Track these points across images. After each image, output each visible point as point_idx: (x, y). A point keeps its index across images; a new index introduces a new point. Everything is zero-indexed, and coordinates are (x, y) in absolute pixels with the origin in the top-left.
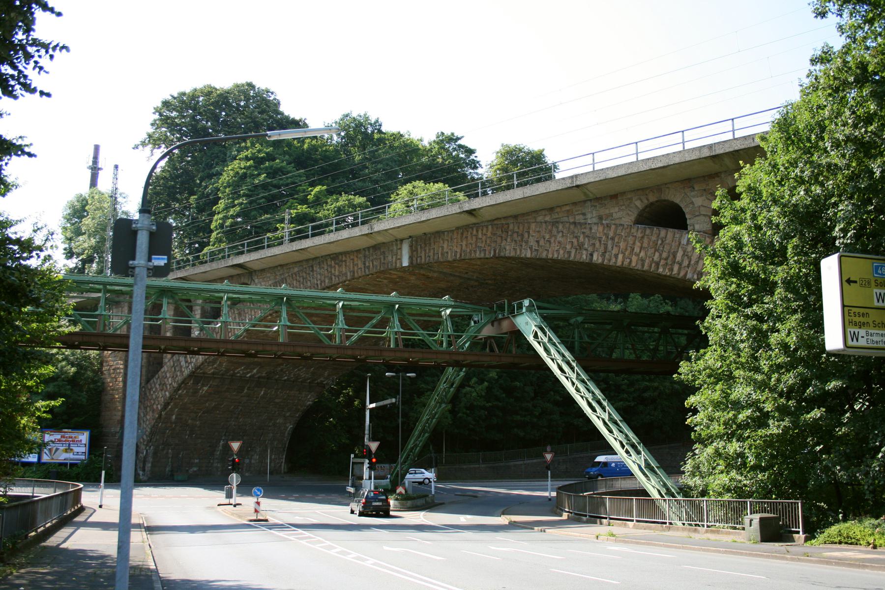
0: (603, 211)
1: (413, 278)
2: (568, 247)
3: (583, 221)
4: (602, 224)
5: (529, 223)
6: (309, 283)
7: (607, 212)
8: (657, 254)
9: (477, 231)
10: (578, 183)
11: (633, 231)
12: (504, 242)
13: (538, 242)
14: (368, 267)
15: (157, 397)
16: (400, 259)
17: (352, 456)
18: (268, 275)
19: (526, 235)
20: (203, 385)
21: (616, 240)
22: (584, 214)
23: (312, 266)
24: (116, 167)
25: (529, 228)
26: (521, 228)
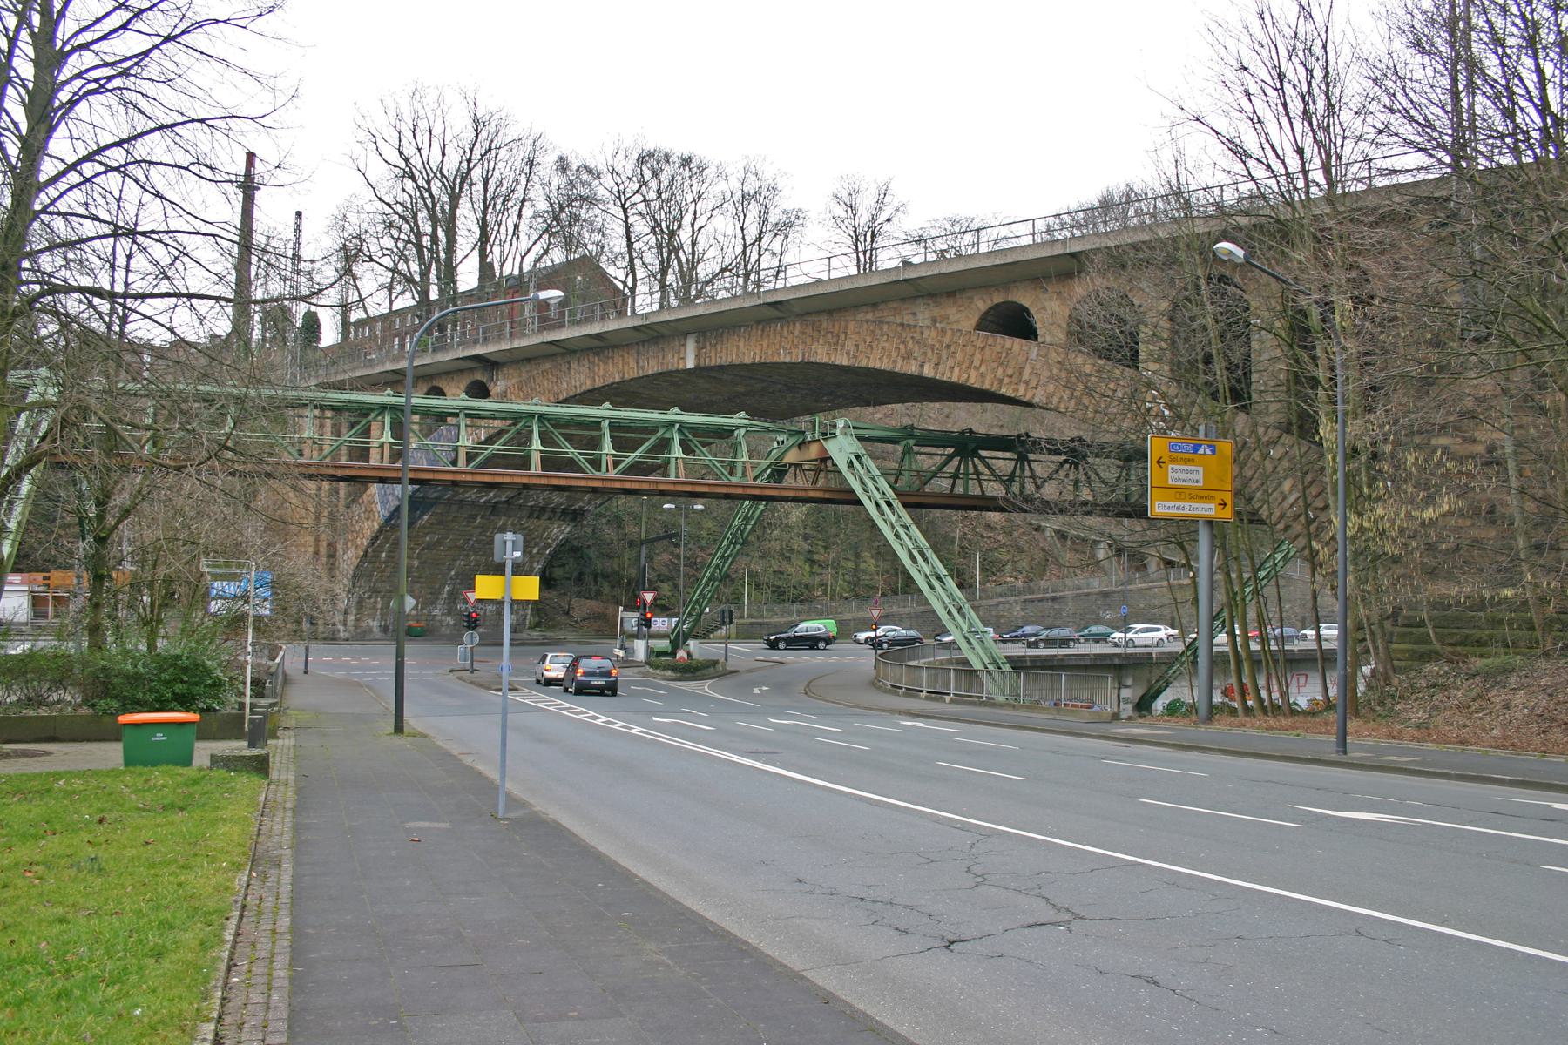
0: (937, 312)
1: (701, 381)
2: (894, 354)
3: (912, 323)
4: (936, 328)
5: (846, 321)
6: (565, 384)
7: (943, 313)
8: (1000, 370)
9: (782, 327)
10: (907, 277)
11: (973, 338)
12: (815, 345)
13: (857, 346)
14: (643, 368)
15: (362, 529)
17: (621, 609)
19: (842, 337)
20: (423, 513)
21: (952, 349)
22: (914, 314)
23: (569, 363)
24: (299, 214)
25: (846, 328)
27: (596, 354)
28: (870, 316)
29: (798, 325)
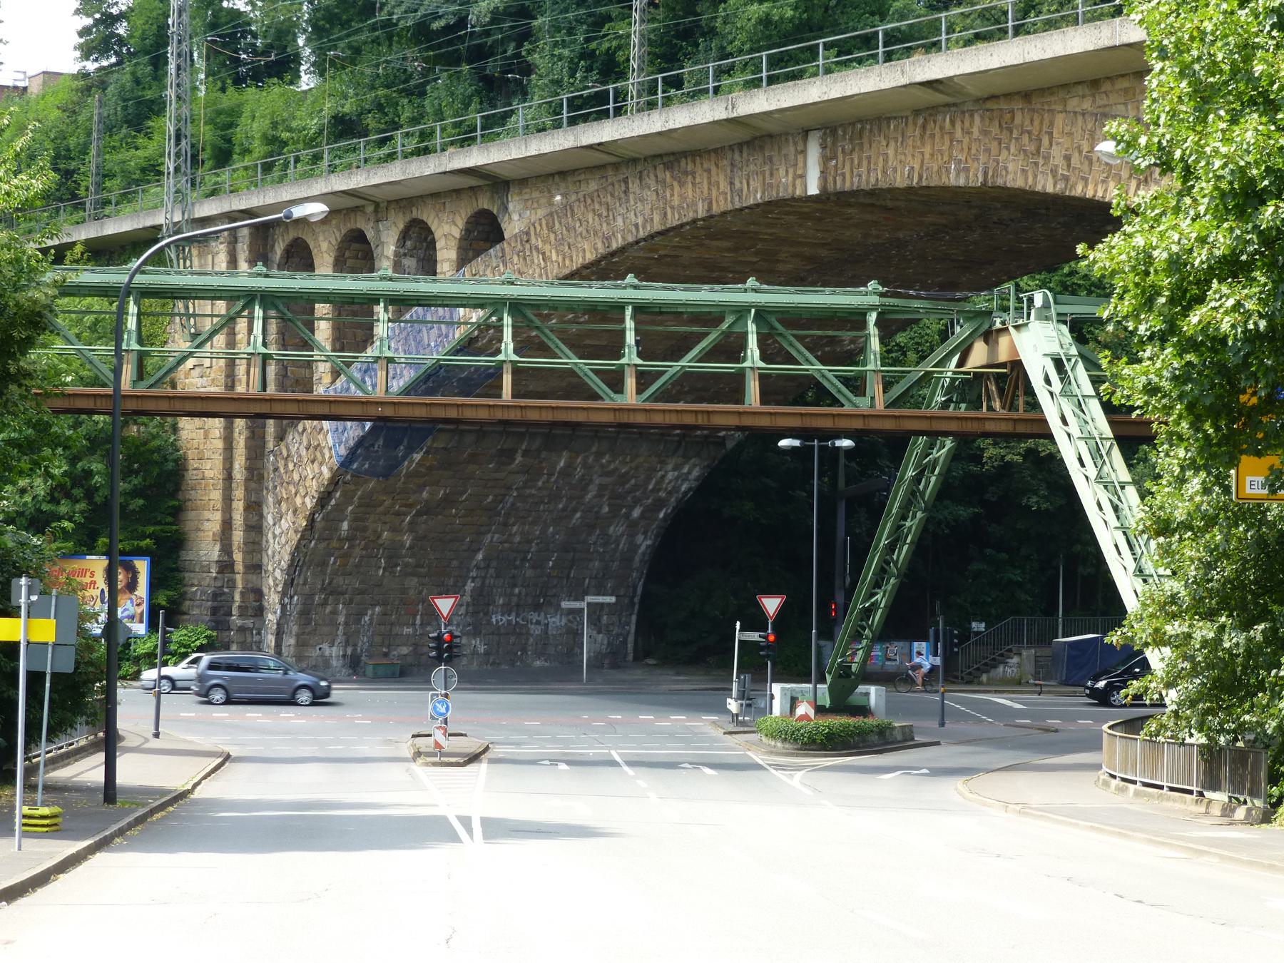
9: (953, 123)
12: (1004, 153)
13: (1068, 158)
16: (803, 177)
18: (536, 194)
23: (626, 181)
25: (1051, 124)
26: (1036, 123)
27: (668, 166)
28: (1087, 105)
29: (977, 118)
